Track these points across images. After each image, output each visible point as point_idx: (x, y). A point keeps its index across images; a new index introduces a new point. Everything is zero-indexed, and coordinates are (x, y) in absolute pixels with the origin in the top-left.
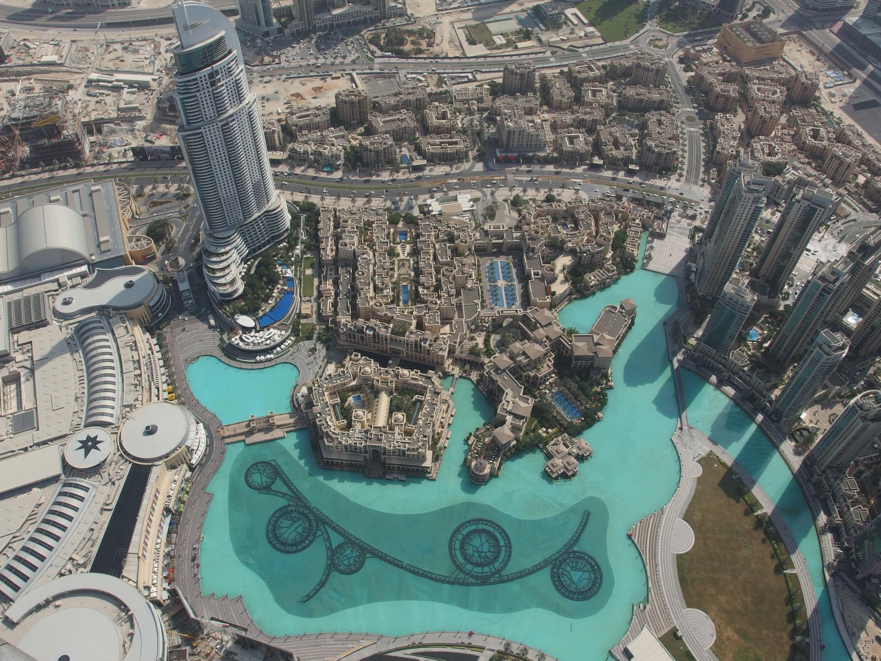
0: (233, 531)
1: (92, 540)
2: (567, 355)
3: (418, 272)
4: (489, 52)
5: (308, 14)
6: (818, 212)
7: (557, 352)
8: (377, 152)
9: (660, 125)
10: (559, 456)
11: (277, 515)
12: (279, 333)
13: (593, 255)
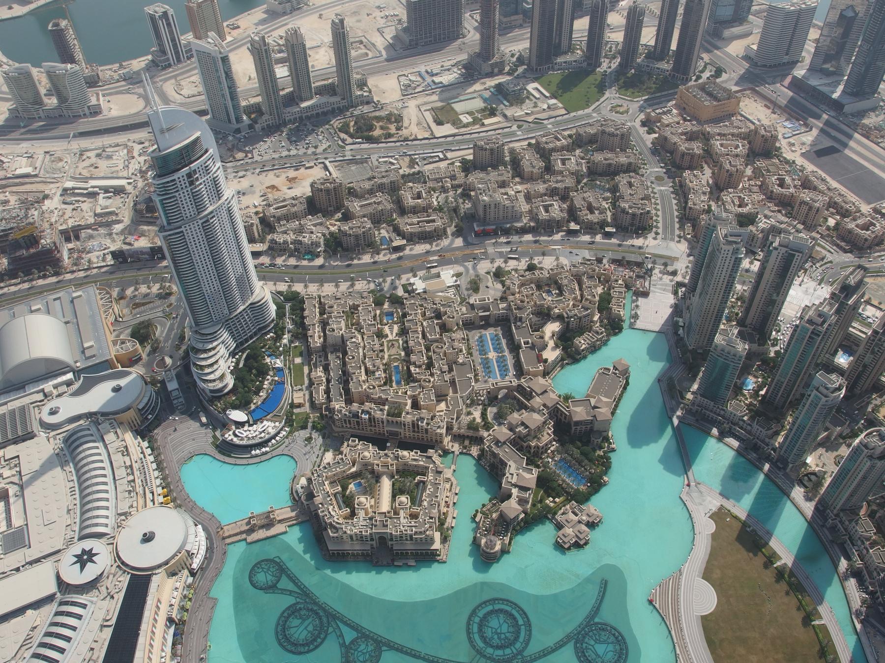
0: (241, 636)
1: (93, 660)
2: (566, 421)
3: (408, 351)
4: (457, 131)
5: (277, 109)
6: (796, 257)
7: (555, 419)
8: (357, 237)
9: (631, 187)
10: (569, 525)
11: (286, 614)
12: (273, 424)
13: (580, 318)
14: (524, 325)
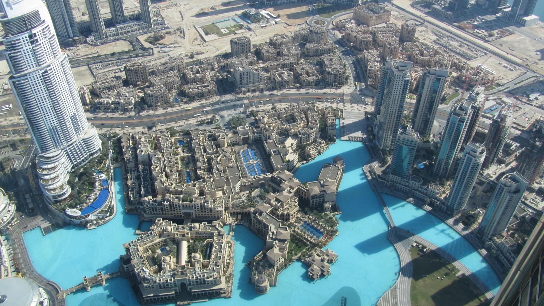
2: (306, 198)
4: (220, 37)
13: (309, 134)
14: (271, 141)
